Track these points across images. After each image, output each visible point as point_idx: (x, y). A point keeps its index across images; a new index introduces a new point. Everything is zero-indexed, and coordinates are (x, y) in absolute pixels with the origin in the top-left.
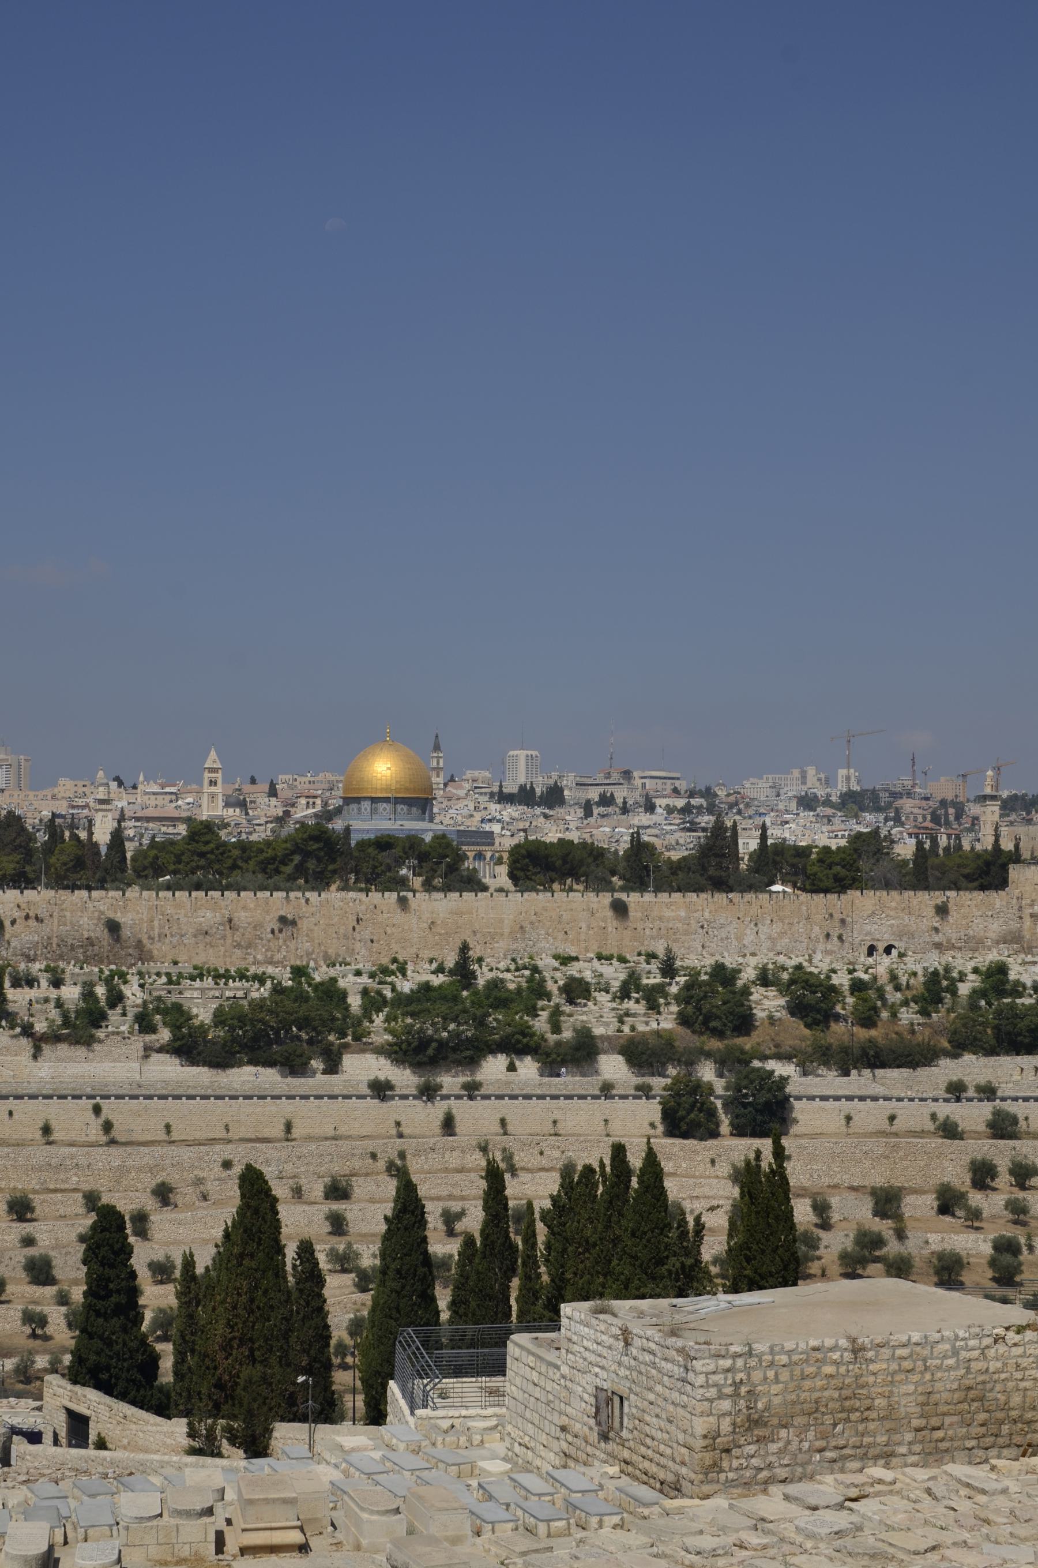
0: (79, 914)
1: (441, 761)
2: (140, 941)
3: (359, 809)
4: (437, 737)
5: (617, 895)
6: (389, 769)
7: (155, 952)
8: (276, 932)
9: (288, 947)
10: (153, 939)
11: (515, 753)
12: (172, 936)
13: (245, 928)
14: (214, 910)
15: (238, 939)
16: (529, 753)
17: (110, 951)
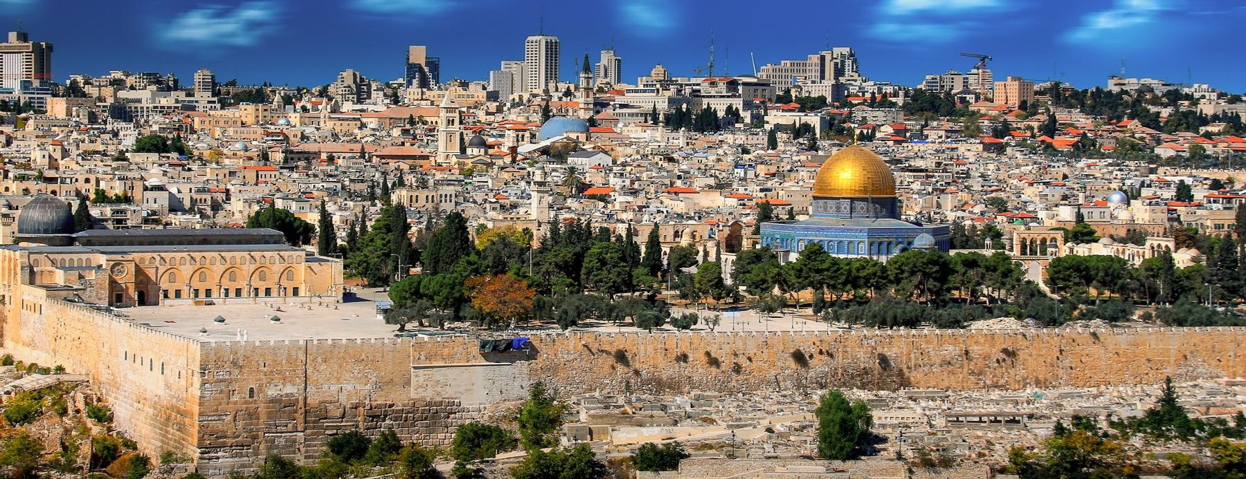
2: (901, 370)
3: (838, 208)
16: (549, 39)
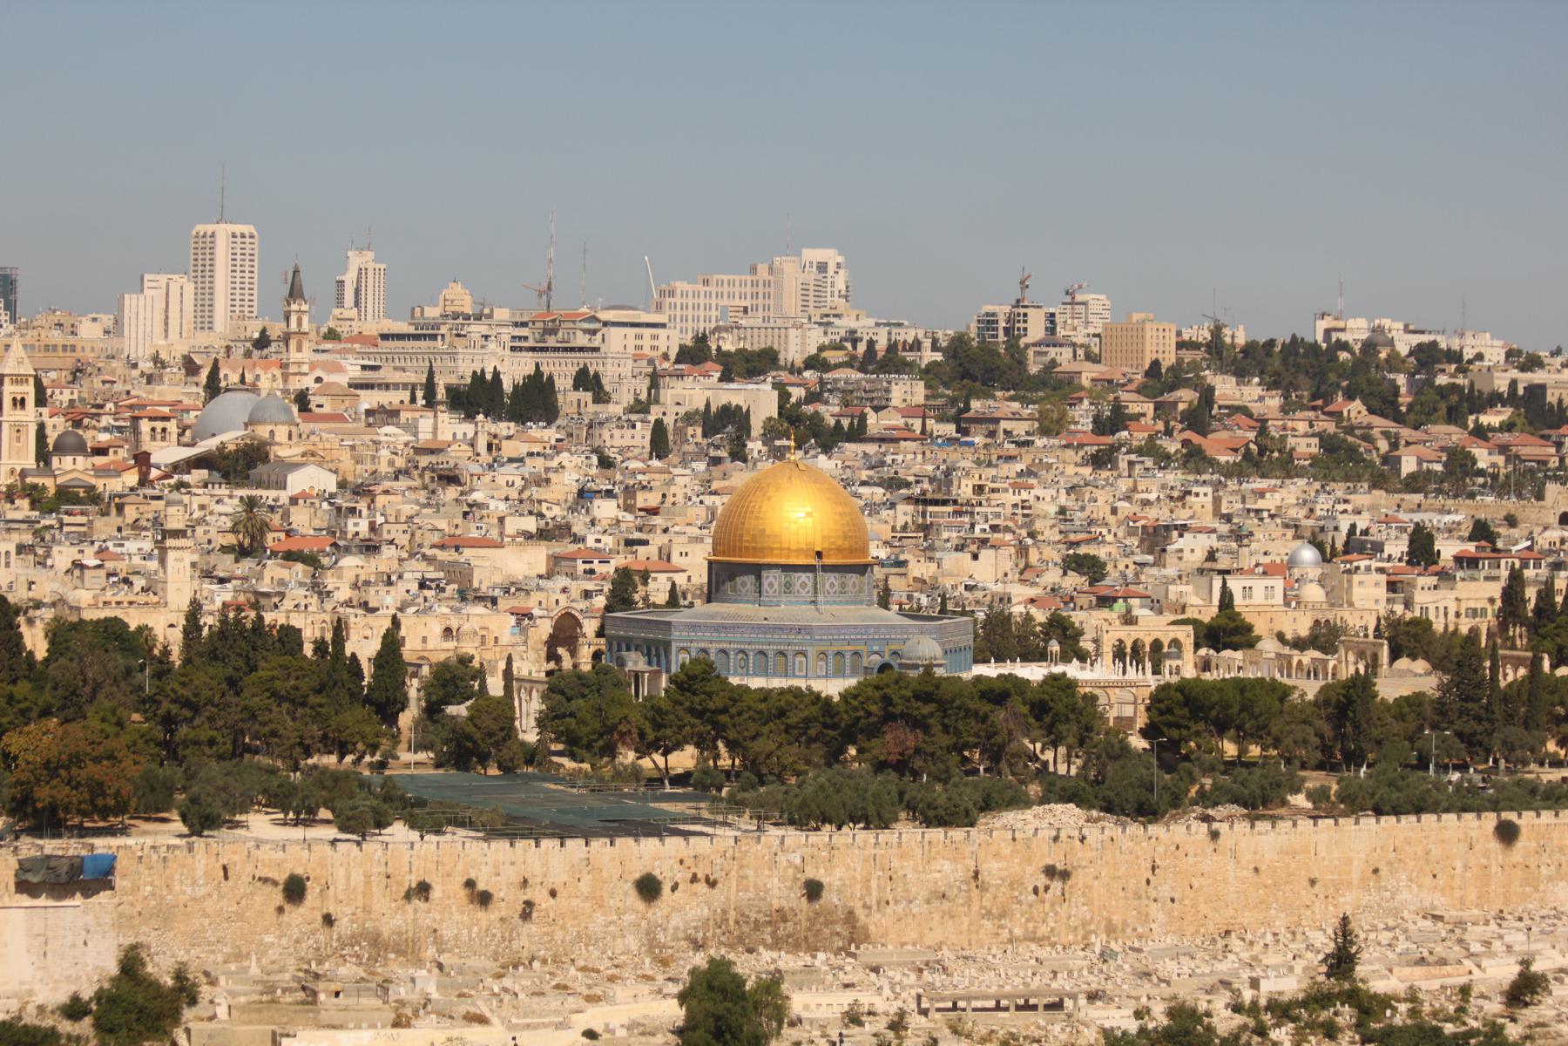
0: (767, 872)
1: (305, 319)
2: (851, 912)
4: (296, 272)
5: (1506, 815)
6: (809, 514)
7: (872, 928)
8: (1041, 889)
9: (1056, 913)
10: (869, 908)
11: (209, 228)
12: (896, 902)
13: (998, 887)
14: (954, 860)
15: (988, 904)
16: (238, 229)
17: (809, 929)
